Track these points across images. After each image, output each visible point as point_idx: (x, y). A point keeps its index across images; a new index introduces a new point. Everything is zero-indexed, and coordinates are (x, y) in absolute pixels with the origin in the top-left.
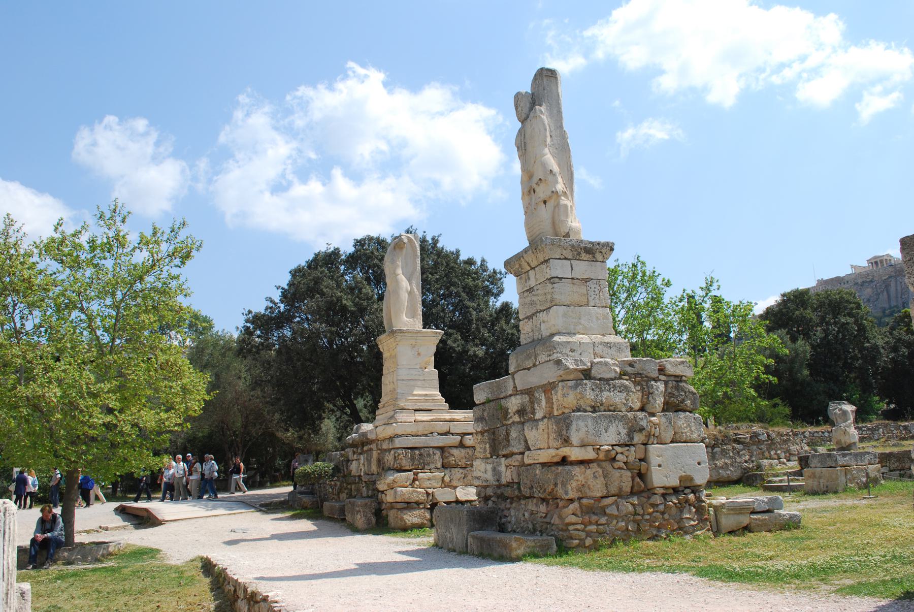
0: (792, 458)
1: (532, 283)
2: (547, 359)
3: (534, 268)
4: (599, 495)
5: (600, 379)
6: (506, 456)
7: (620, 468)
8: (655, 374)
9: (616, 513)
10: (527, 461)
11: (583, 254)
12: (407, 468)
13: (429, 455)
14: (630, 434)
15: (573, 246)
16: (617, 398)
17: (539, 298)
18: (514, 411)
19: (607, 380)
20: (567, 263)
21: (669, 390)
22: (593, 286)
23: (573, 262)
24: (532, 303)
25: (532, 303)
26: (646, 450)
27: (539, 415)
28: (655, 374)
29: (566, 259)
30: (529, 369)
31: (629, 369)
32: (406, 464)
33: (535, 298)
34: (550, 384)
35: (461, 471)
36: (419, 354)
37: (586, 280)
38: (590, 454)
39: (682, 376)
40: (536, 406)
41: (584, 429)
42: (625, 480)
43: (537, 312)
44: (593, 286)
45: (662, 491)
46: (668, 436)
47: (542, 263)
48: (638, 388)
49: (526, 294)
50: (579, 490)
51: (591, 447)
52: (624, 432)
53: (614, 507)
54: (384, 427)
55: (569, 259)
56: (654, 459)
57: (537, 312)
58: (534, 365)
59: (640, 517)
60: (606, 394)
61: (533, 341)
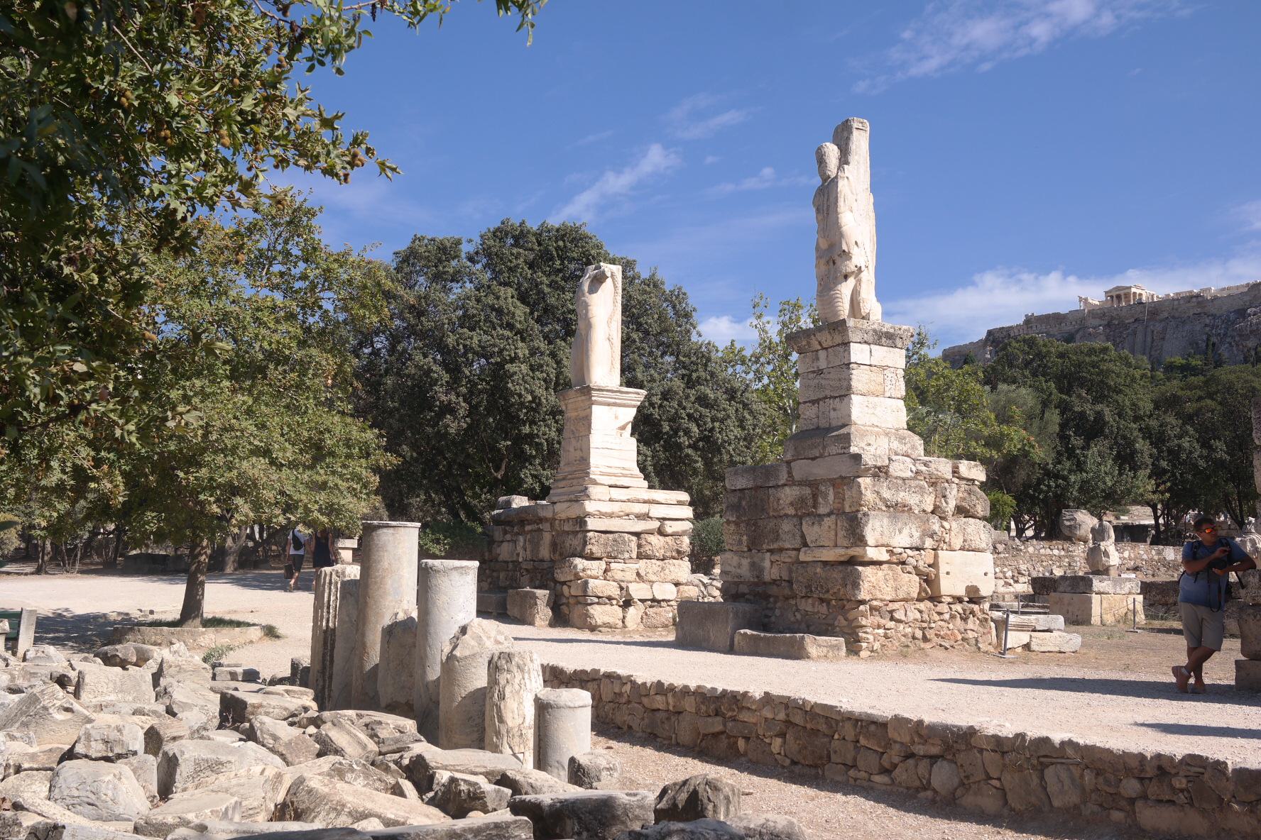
0: (1022, 579)
1: (822, 364)
2: (840, 451)
3: (826, 349)
4: (889, 598)
5: (896, 478)
6: (771, 551)
7: (909, 573)
8: (949, 476)
9: (903, 618)
10: (802, 557)
11: (884, 340)
12: (598, 555)
13: (624, 541)
14: (922, 538)
15: (874, 331)
16: (912, 499)
17: (831, 383)
18: (788, 502)
19: (904, 479)
20: (866, 347)
21: (961, 495)
22: (890, 375)
23: (872, 346)
24: (819, 386)
25: (819, 386)
26: (936, 557)
27: (822, 510)
28: (949, 476)
29: (865, 342)
30: (813, 459)
31: (923, 468)
32: (596, 549)
33: (823, 382)
34: (842, 478)
35: (659, 563)
36: (616, 417)
37: (883, 368)
38: (885, 556)
39: (974, 480)
40: (820, 500)
41: (879, 529)
42: (912, 584)
43: (826, 398)
44: (890, 375)
45: (950, 600)
46: (957, 543)
47: (838, 345)
48: (931, 489)
49: (811, 376)
50: (870, 592)
51: (884, 549)
52: (917, 535)
53: (903, 612)
54: (569, 504)
55: (869, 344)
56: (943, 568)
57: (826, 398)
58: (821, 456)
59: (925, 625)
60: (902, 494)
61: (818, 428)
